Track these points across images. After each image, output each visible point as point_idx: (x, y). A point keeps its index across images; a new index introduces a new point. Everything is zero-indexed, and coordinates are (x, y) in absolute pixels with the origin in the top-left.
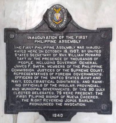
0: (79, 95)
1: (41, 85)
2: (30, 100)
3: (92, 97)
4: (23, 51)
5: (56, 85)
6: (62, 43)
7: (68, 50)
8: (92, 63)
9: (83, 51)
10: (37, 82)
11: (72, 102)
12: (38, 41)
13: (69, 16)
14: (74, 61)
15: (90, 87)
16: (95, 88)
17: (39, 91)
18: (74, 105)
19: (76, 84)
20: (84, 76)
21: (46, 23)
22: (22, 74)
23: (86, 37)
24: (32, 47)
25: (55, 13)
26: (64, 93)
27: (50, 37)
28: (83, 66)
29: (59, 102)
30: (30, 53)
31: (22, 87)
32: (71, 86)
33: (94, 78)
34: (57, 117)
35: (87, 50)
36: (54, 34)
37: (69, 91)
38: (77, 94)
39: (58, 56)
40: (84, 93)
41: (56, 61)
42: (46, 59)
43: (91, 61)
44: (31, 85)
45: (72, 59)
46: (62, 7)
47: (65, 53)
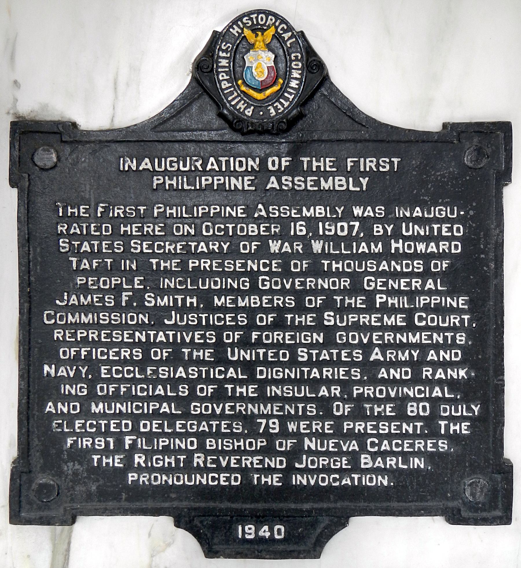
1: (184, 391)
10: (164, 372)
14: (339, 274)
17: (171, 418)
22: (93, 335)
26: (292, 427)
28: (379, 299)
29: (270, 471)
37: (317, 417)
41: (253, 275)
44: (137, 390)
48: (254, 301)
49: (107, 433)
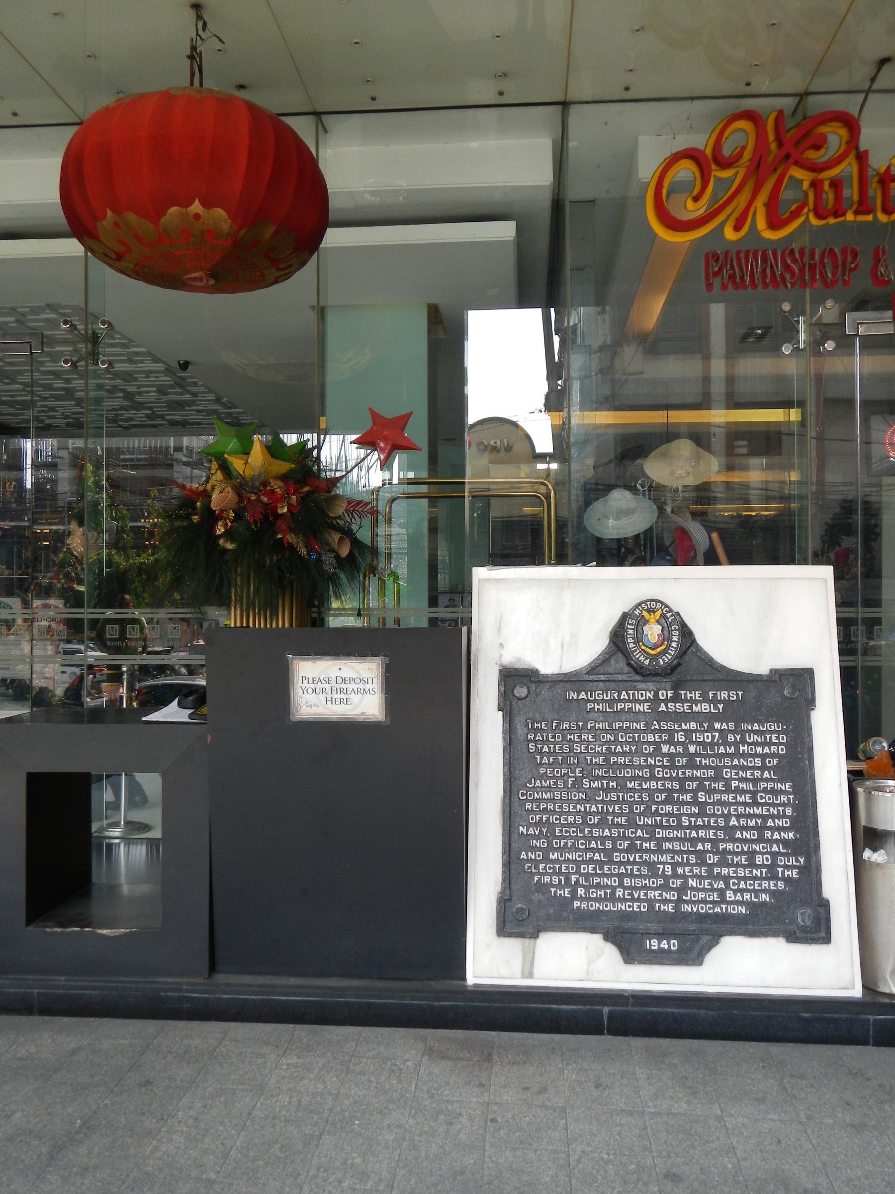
0: (726, 879)
1: (609, 845)
3: (765, 884)
4: (553, 737)
6: (668, 712)
7: (688, 733)
8: (762, 774)
9: (731, 738)
10: (596, 832)
12: (597, 707)
13: (686, 633)
14: (707, 767)
15: (760, 853)
16: (774, 855)
17: (601, 864)
18: (711, 911)
19: (715, 842)
20: (738, 817)
21: (620, 655)
22: (550, 807)
23: (737, 695)
24: (580, 724)
25: (645, 624)
26: (680, 871)
27: (634, 694)
28: (734, 784)
29: (666, 901)
31: (550, 848)
33: (770, 823)
34: (661, 951)
35: (743, 733)
36: (643, 685)
37: (696, 864)
38: (719, 874)
39: (657, 752)
40: (741, 873)
41: (651, 767)
42: (621, 760)
43: (758, 768)
44: (579, 844)
45: (701, 761)
46: (667, 606)
47: (679, 743)
48: (653, 784)
49: (560, 873)
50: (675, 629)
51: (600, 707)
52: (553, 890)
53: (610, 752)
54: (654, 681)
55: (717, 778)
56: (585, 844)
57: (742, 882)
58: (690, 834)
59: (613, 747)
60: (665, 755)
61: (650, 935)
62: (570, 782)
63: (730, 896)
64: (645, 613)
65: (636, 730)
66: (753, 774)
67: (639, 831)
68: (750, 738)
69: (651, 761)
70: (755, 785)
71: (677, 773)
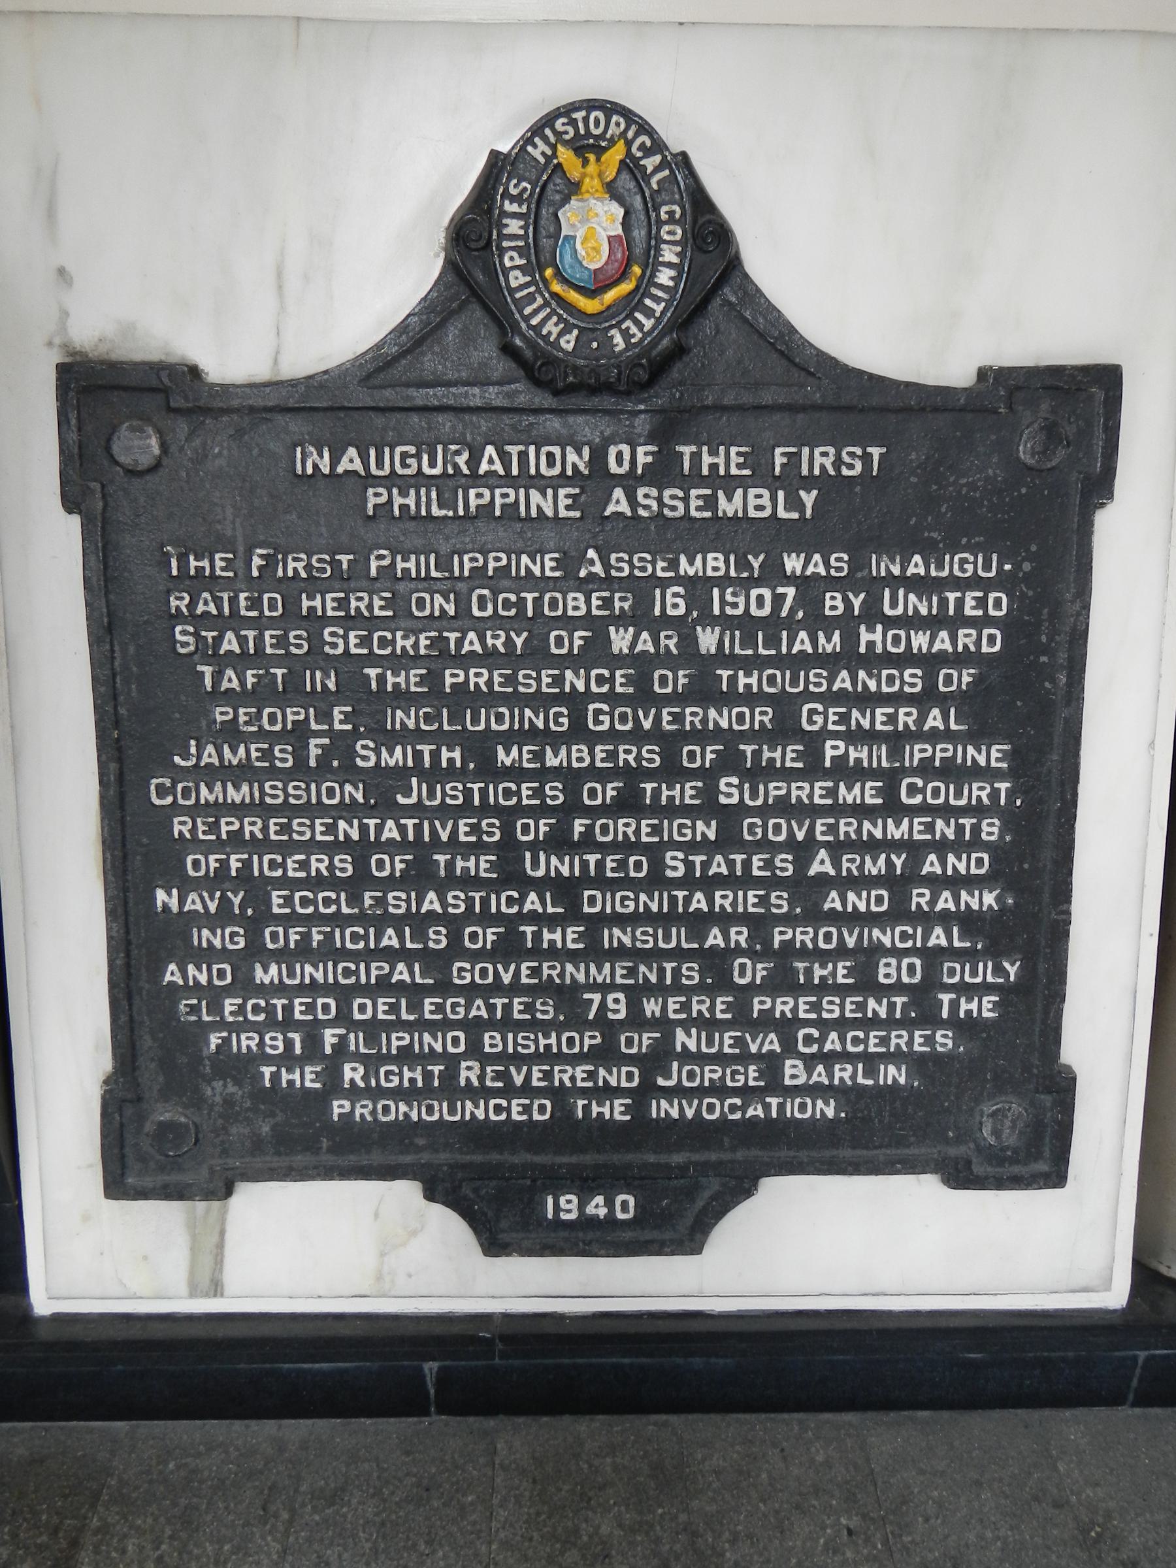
0: (787, 1027)
1: (438, 939)
2: (332, 1076)
3: (898, 1039)
4: (255, 603)
5: (572, 932)
6: (636, 517)
7: (697, 588)
8: (922, 719)
9: (833, 603)
10: (397, 902)
11: (719, 1090)
12: (398, 501)
13: (710, 235)
14: (752, 698)
15: (895, 952)
16: (933, 957)
17: (415, 993)
18: (737, 1116)
19: (759, 925)
20: (837, 849)
21: (479, 313)
22: (252, 827)
23: (866, 458)
24: (345, 559)
25: (566, 200)
26: (651, 1007)
27: (523, 456)
28: (831, 750)
29: (608, 1092)
30: (325, 620)
31: (255, 951)
32: (715, 938)
33: (931, 865)
34: (587, 1223)
35: (874, 586)
36: (554, 424)
37: (701, 988)
39: (596, 652)
40: (831, 1009)
41: (576, 702)
42: (478, 678)
43: (911, 700)
44: (345, 938)
45: (733, 680)
46: (644, 128)
47: (666, 621)
48: (578, 755)
49: (289, 1023)
50: (672, 220)
51: (411, 501)
52: (267, 1071)
53: (444, 653)
54: (593, 411)
55: (785, 729)
56: (366, 938)
57: (834, 1035)
58: (687, 901)
59: (453, 636)
60: (619, 660)
61: (557, 1182)
62: (314, 752)
63: (793, 1072)
64: (565, 155)
65: (530, 580)
66: (892, 719)
67: (533, 896)
68: (894, 604)
69: (574, 680)
70: (895, 753)
71: (658, 719)
